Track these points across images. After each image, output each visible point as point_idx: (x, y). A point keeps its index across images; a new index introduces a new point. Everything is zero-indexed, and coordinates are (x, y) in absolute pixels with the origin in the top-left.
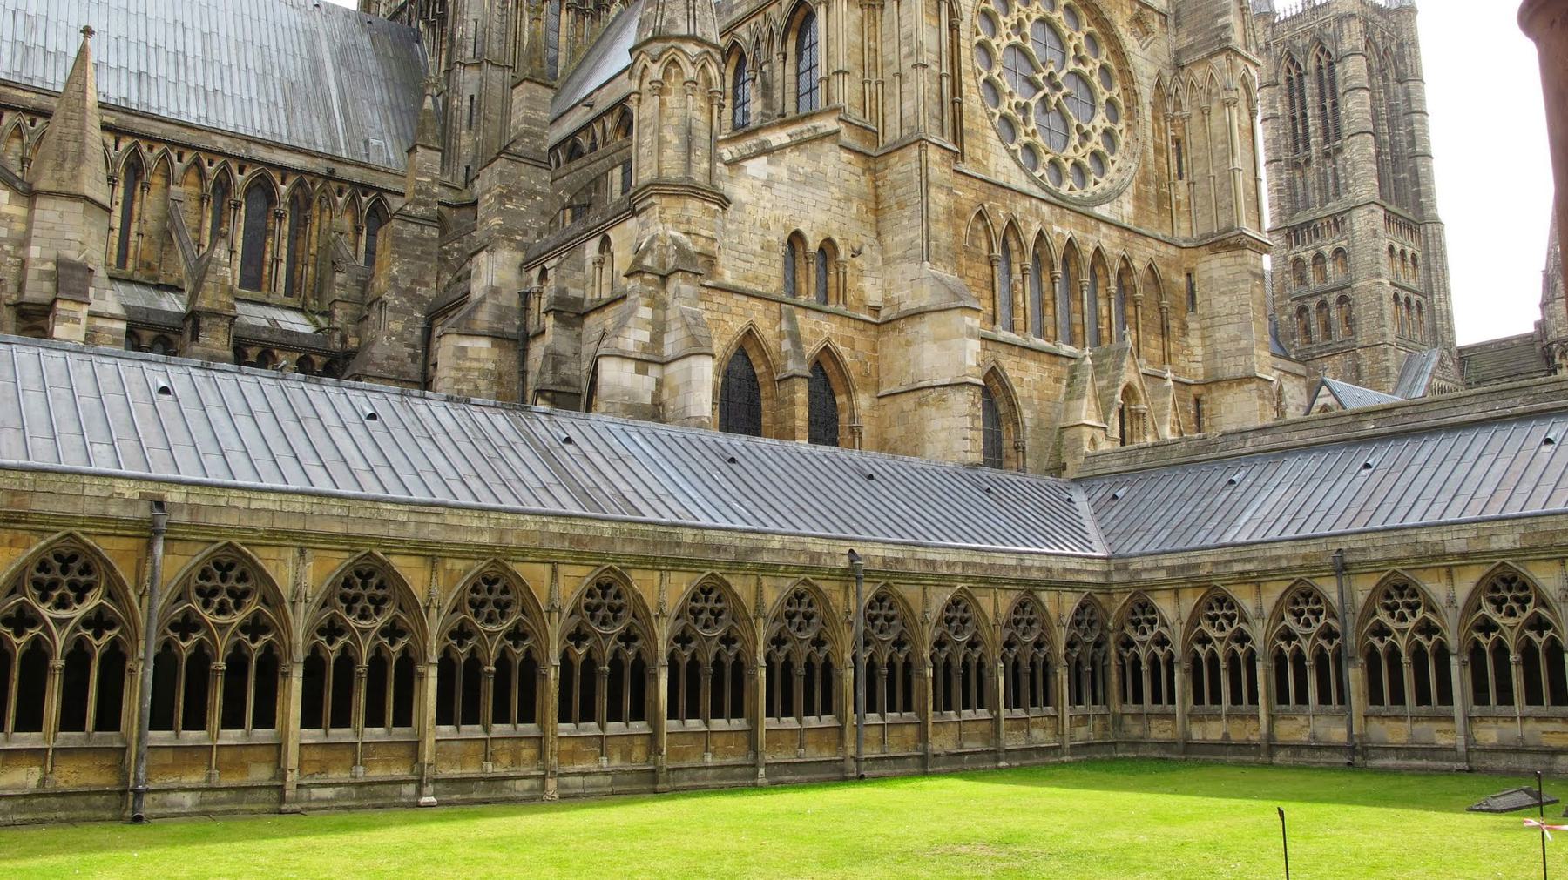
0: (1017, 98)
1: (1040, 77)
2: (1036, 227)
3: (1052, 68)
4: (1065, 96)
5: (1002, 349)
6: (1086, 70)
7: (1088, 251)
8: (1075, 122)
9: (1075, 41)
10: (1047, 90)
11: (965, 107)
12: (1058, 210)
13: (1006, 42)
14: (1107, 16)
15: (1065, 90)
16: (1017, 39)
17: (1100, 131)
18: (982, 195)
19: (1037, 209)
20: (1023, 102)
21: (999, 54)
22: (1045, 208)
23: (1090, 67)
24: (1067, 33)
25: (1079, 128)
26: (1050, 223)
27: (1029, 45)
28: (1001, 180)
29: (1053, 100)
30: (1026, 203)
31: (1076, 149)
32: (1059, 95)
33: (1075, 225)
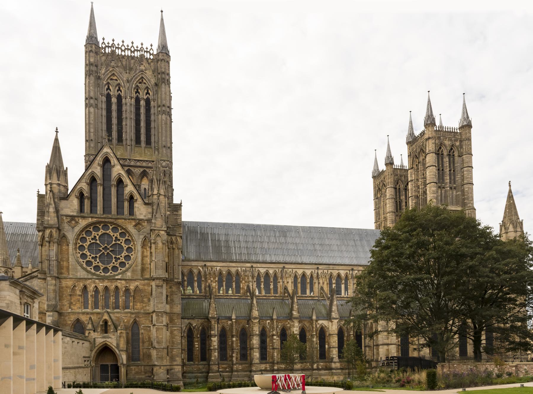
0: (92, 255)
1: (101, 249)
2: (93, 285)
3: (106, 245)
4: (111, 251)
5: (81, 315)
6: (119, 242)
7: (113, 287)
8: (114, 256)
9: (115, 236)
10: (103, 251)
11: (70, 263)
12: (102, 280)
13: (89, 243)
14: (124, 227)
15: (111, 249)
16: (94, 241)
17: (123, 256)
18: (75, 282)
19: (94, 281)
20: (94, 256)
21: (86, 247)
22: (97, 281)
23: (121, 241)
24: (112, 235)
25: (115, 258)
26: (99, 284)
27: (98, 242)
28: (82, 277)
29: (106, 253)
30: (91, 281)
31: (114, 263)
32: (108, 251)
33: (108, 282)
